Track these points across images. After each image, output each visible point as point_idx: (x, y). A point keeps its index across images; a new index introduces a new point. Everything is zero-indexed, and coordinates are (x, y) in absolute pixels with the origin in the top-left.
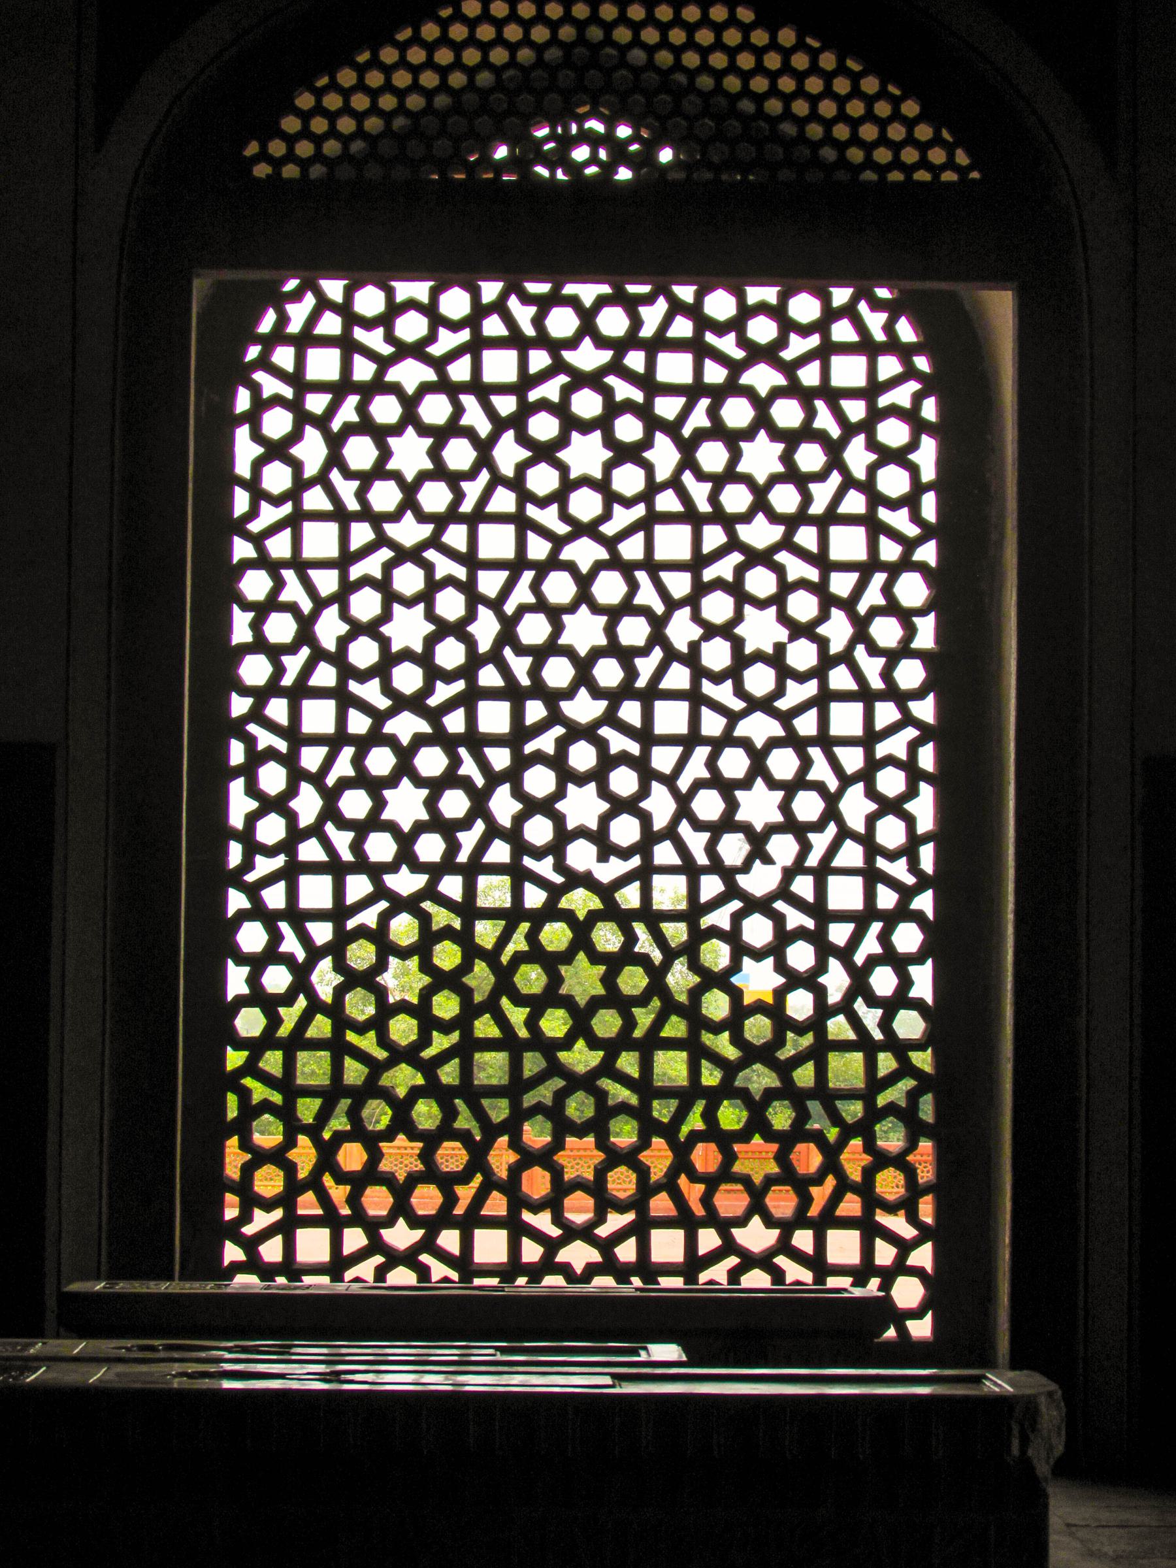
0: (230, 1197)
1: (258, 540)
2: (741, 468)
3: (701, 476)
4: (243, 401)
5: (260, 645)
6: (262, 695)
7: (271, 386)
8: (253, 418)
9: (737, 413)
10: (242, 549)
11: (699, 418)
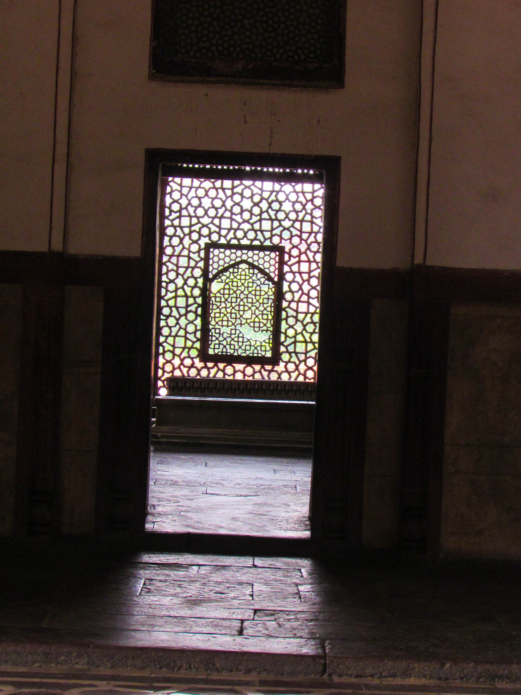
0: (159, 370)
1: (172, 221)
2: (282, 208)
3: (273, 210)
4: (168, 189)
5: (171, 245)
6: (171, 256)
7: (175, 187)
8: (170, 193)
9: (281, 197)
10: (167, 222)
11: (273, 197)
